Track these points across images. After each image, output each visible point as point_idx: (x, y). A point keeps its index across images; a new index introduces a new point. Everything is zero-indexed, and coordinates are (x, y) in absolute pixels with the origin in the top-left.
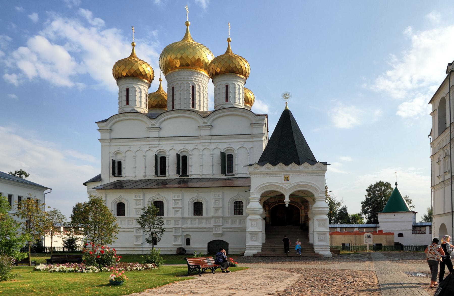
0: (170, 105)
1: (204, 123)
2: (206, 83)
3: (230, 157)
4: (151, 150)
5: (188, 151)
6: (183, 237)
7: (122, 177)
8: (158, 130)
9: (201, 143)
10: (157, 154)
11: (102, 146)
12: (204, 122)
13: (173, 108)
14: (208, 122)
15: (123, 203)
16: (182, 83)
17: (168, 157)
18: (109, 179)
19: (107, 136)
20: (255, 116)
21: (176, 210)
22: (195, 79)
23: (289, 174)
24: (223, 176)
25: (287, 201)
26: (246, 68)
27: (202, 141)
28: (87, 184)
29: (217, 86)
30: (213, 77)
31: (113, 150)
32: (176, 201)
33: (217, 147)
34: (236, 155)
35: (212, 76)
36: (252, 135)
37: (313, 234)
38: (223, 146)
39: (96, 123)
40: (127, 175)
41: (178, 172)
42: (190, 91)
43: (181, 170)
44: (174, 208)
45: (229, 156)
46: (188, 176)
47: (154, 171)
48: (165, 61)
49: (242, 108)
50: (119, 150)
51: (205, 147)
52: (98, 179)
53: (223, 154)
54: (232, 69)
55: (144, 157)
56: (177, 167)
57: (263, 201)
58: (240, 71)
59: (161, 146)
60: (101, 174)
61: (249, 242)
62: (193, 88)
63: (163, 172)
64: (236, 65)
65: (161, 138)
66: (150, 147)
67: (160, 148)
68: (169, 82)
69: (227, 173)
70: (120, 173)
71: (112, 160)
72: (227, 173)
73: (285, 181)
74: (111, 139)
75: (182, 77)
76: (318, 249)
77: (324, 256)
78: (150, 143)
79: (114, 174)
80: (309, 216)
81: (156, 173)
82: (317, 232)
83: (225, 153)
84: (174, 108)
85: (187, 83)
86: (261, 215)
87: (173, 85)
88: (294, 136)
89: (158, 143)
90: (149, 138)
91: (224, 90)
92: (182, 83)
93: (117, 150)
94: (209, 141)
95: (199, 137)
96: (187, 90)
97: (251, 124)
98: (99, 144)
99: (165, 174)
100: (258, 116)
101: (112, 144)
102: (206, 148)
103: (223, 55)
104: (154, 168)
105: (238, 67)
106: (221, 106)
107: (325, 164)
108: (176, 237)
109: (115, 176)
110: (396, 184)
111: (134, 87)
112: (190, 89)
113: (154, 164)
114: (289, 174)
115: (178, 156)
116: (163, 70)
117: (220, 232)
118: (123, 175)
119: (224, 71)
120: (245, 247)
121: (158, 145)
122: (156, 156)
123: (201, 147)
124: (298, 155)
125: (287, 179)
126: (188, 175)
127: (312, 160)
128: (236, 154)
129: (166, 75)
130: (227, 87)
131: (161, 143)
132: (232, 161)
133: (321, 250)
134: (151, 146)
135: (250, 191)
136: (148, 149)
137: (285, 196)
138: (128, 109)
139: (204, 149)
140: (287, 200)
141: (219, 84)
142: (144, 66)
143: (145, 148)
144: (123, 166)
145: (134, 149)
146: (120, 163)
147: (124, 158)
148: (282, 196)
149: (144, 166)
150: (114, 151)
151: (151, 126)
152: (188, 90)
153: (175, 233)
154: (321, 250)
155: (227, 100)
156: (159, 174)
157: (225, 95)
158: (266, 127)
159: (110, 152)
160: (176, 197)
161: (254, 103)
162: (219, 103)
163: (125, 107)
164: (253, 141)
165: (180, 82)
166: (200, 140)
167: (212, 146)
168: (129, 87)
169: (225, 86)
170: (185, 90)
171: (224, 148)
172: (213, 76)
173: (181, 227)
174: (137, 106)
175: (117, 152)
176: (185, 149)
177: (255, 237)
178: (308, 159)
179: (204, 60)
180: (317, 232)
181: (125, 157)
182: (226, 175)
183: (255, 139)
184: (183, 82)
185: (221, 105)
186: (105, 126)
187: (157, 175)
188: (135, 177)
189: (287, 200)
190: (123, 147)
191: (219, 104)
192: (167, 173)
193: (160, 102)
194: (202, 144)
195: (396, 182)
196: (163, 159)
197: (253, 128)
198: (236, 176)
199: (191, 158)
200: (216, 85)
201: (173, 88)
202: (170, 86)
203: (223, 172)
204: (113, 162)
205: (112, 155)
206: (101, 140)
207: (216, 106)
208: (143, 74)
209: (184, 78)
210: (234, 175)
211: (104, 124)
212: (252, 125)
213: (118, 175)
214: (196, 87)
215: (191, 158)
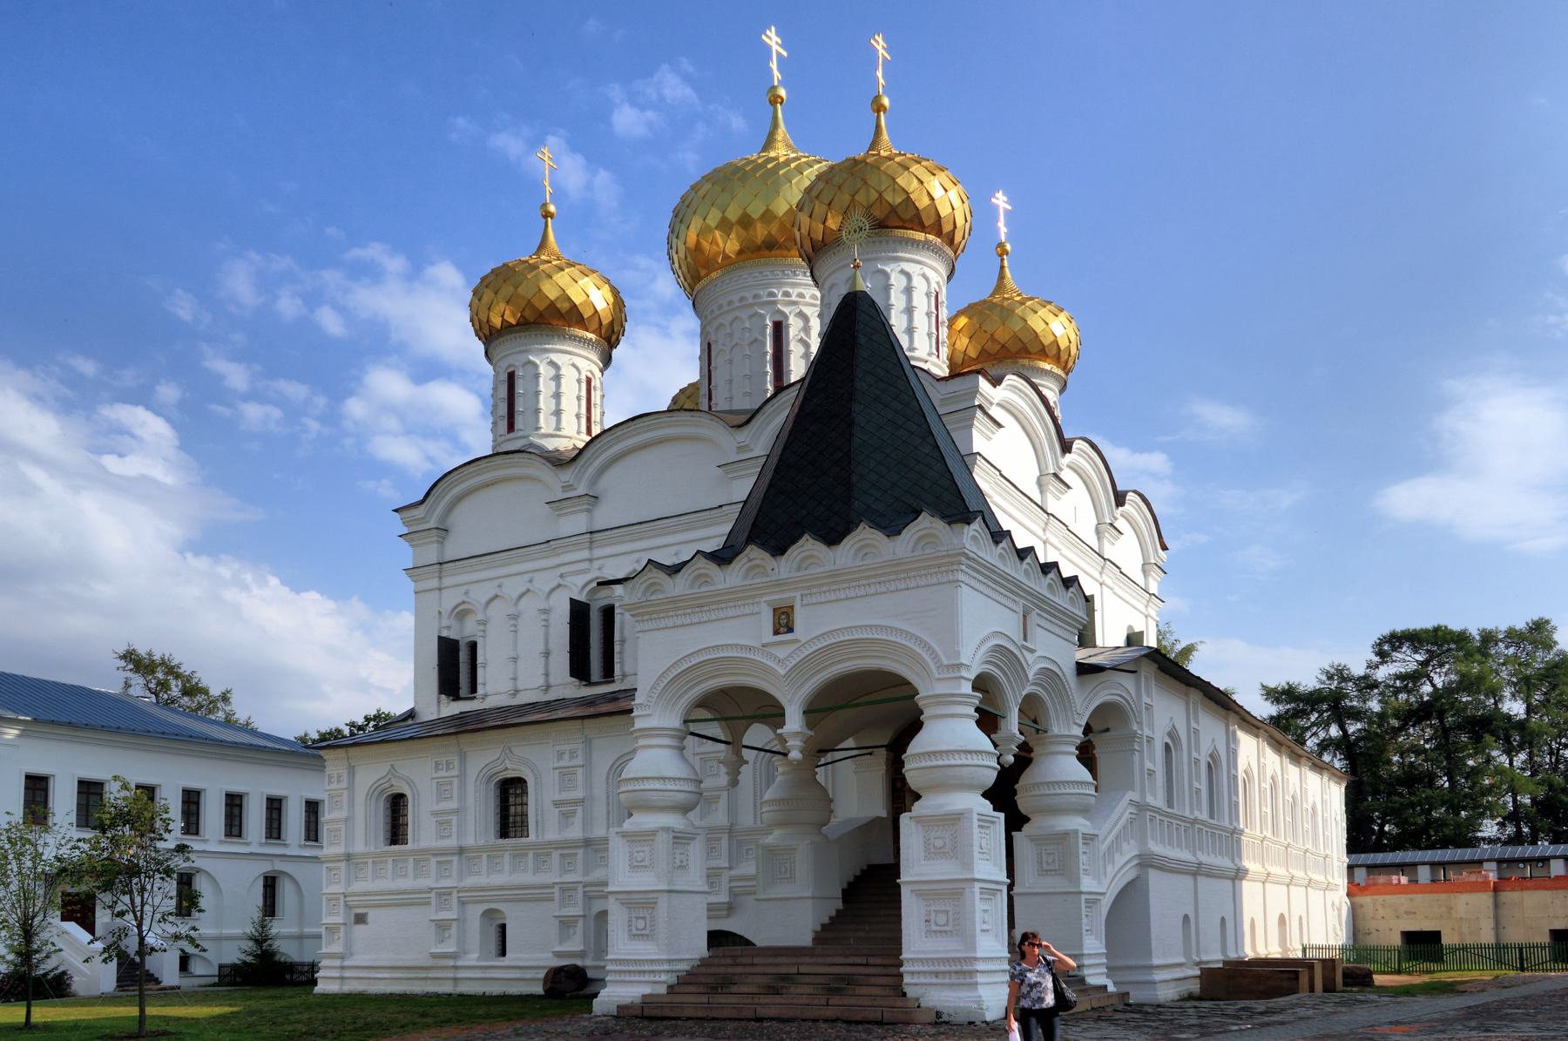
1: (741, 449)
6: (592, 924)
8: (586, 507)
12: (738, 448)
16: (736, 318)
21: (566, 810)
22: (787, 294)
23: (792, 594)
31: (451, 599)
32: (566, 775)
39: (396, 511)
40: (490, 689)
42: (764, 344)
44: (557, 804)
50: (466, 600)
55: (544, 617)
59: (596, 564)
61: (621, 946)
62: (779, 329)
65: (595, 535)
66: (561, 576)
73: (776, 633)
75: (735, 298)
76: (922, 980)
77: (945, 1018)
78: (561, 559)
82: (916, 887)
85: (751, 317)
89: (585, 554)
93: (460, 600)
101: (447, 581)
108: (566, 924)
111: (530, 362)
112: (764, 336)
114: (792, 594)
121: (586, 565)
125: (783, 622)
131: (597, 552)
133: (934, 980)
134: (563, 570)
136: (555, 584)
142: (562, 279)
143: (545, 582)
145: (513, 588)
146: (473, 647)
147: (481, 627)
149: (541, 648)
152: (756, 340)
153: (563, 905)
154: (934, 980)
159: (440, 613)
160: (566, 756)
163: (505, 441)
173: (580, 879)
174: (543, 431)
177: (644, 918)
180: (916, 887)
184: (737, 313)
186: (422, 520)
188: (515, 694)
190: (475, 587)
205: (445, 622)
208: (564, 306)
209: (742, 299)
211: (419, 512)
214: (788, 326)
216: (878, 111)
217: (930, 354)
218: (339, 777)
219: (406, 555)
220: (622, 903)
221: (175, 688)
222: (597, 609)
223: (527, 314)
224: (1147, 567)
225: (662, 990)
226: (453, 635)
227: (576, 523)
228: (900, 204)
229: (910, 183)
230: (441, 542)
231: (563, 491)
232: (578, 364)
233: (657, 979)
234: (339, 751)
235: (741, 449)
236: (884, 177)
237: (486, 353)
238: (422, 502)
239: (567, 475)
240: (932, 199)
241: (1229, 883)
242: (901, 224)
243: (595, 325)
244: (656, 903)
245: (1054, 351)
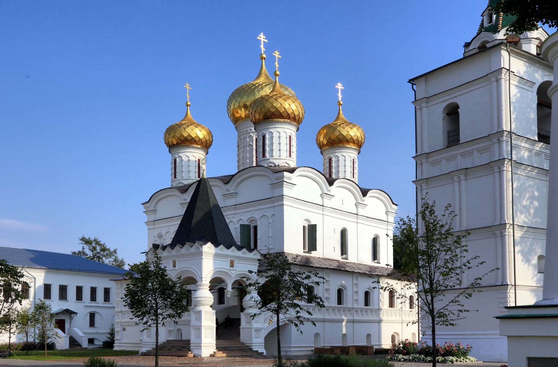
16: (245, 137)
31: (156, 232)
58: (277, 114)
75: (245, 130)
94: (234, 212)
120: (188, 343)
150: (157, 234)
159: (154, 236)
164: (274, 207)
166: (226, 212)
171: (247, 219)
175: (160, 234)
184: (245, 135)
186: (149, 207)
208: (189, 138)
211: (148, 205)
216: (276, 76)
217: (287, 157)
218: (119, 288)
219: (145, 218)
221: (98, 249)
223: (179, 141)
224: (387, 213)
226: (157, 243)
228: (275, 111)
229: (278, 104)
230: (155, 214)
232: (195, 155)
234: (118, 281)
236: (269, 103)
237: (169, 151)
238: (149, 202)
240: (285, 109)
241: (378, 324)
242: (276, 117)
243: (200, 142)
245: (352, 140)
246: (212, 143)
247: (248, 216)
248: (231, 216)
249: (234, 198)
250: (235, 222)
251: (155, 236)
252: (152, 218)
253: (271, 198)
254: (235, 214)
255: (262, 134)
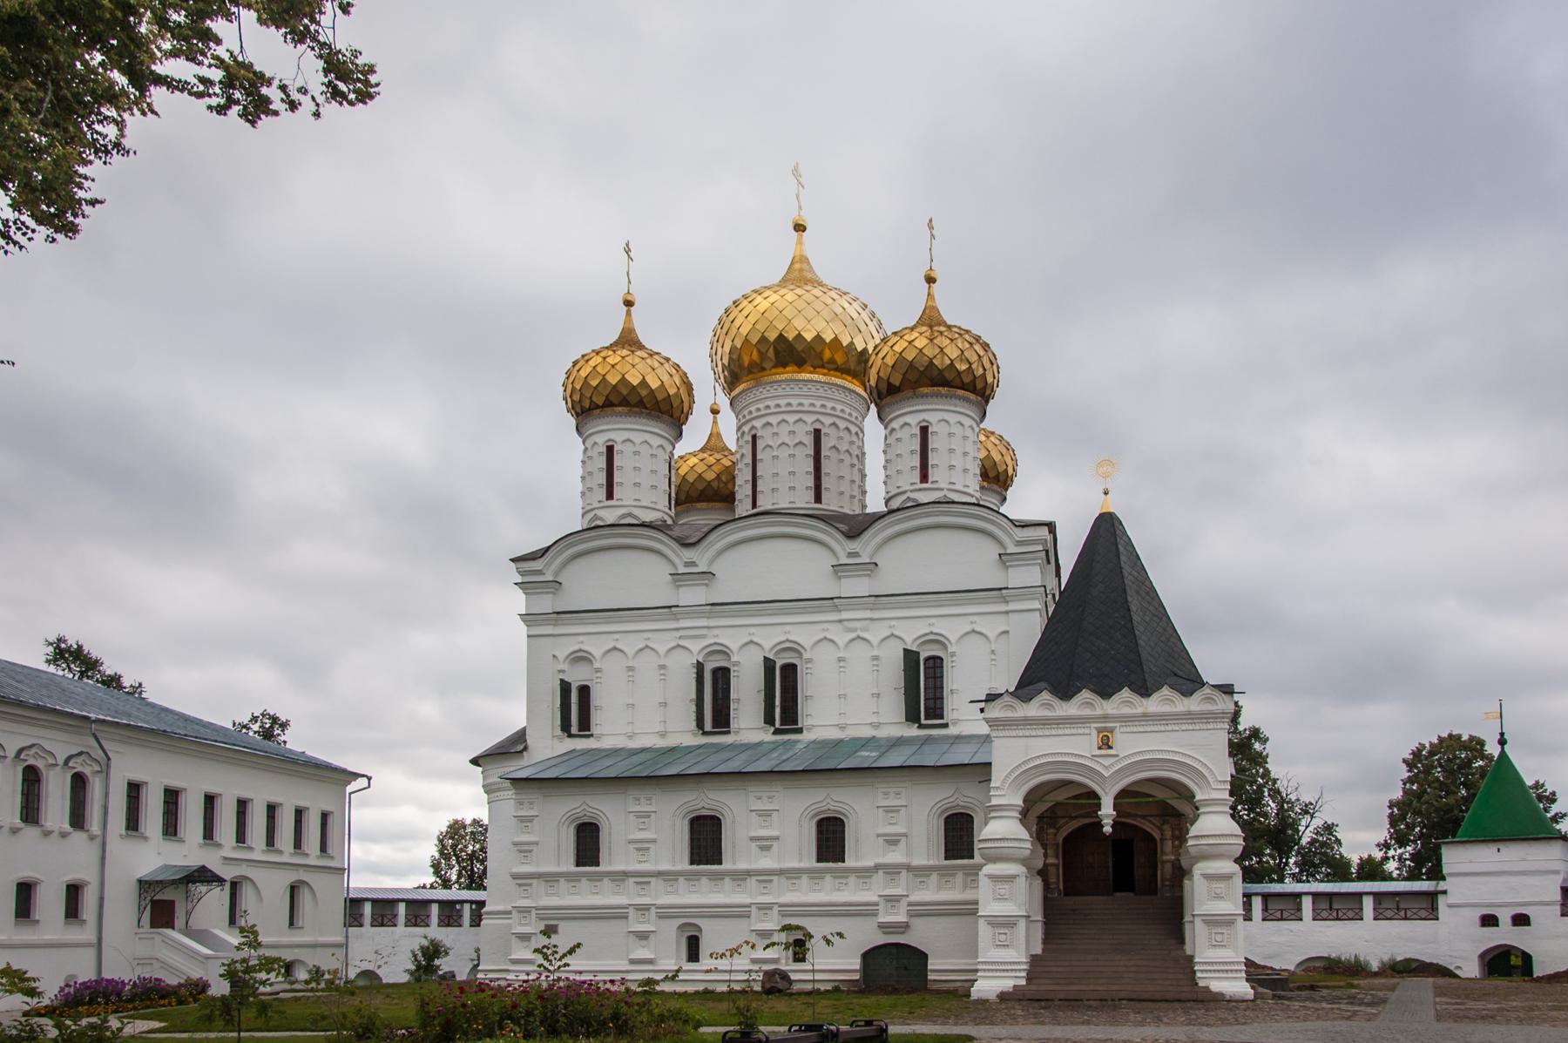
0: (743, 491)
2: (860, 419)
3: (935, 664)
4: (684, 647)
5: (802, 651)
7: (592, 735)
9: (840, 621)
10: (700, 660)
11: (529, 636)
13: (754, 505)
14: (865, 547)
15: (595, 824)
17: (736, 668)
18: (548, 747)
19: (546, 604)
20: (1012, 527)
24: (913, 731)
25: (1108, 816)
26: (985, 370)
27: (845, 615)
28: (480, 762)
29: (893, 430)
30: (878, 401)
31: (565, 648)
33: (893, 635)
34: (954, 659)
35: (876, 397)
36: (1003, 591)
37: (1192, 922)
38: (912, 631)
41: (769, 720)
43: (778, 711)
45: (931, 663)
46: (800, 731)
47: (694, 716)
48: (727, 349)
49: (973, 500)
51: (853, 635)
52: (514, 746)
53: (910, 657)
54: (941, 372)
56: (765, 701)
57: (1042, 807)
59: (716, 632)
60: (525, 728)
63: (722, 720)
64: (952, 361)
66: (680, 638)
67: (712, 641)
68: (740, 417)
69: (926, 719)
70: (585, 724)
71: (562, 680)
72: (926, 719)
74: (558, 613)
78: (682, 624)
79: (565, 726)
80: (1184, 863)
81: (700, 723)
83: (918, 653)
84: (758, 504)
86: (1024, 862)
87: (753, 427)
88: (1129, 599)
89: (703, 622)
90: (677, 606)
91: (917, 446)
92: (784, 421)
94: (867, 614)
95: (835, 601)
96: (797, 444)
97: (1000, 555)
98: (523, 629)
99: (727, 724)
100: (1023, 526)
102: (859, 637)
103: (912, 329)
104: (694, 708)
105: (958, 367)
106: (903, 497)
107: (1228, 690)
109: (570, 736)
110: (1502, 742)
113: (694, 696)
115: (769, 665)
116: (722, 379)
117: (902, 918)
118: (595, 730)
119: (915, 382)
121: (704, 632)
122: (700, 667)
123: (842, 638)
124: (1141, 663)
126: (800, 726)
127: (1188, 680)
128: (953, 654)
129: (733, 394)
130: (924, 431)
132: (942, 677)
134: (681, 633)
135: (990, 780)
136: (674, 644)
137: (1099, 798)
138: (610, 516)
139: (854, 639)
140: (1107, 811)
141: (895, 425)
144: (596, 699)
146: (585, 691)
148: (1091, 798)
151: (682, 570)
155: (924, 477)
156: (708, 726)
157: (916, 462)
158: (1049, 562)
161: (1015, 479)
162: (898, 487)
164: (1007, 612)
165: (774, 420)
167: (875, 634)
168: (613, 441)
169: (918, 432)
170: (791, 444)
172: (879, 398)
176: (791, 641)
178: (1175, 675)
179: (852, 343)
181: (598, 670)
182: (921, 726)
183: (1012, 606)
184: (786, 417)
185: (905, 492)
187: (703, 730)
189: (1107, 811)
191: (901, 490)
192: (734, 725)
193: (715, 485)
194: (846, 623)
195: (1502, 734)
196: (722, 677)
197: (1007, 567)
198: (952, 730)
199: (809, 671)
200: (889, 428)
201: (754, 437)
202: (744, 432)
203: (912, 716)
204: (565, 687)
206: (527, 617)
207: (890, 495)
210: (946, 726)
212: (1003, 557)
213: (579, 731)
215: (809, 671)
220: (989, 924)
222: (712, 667)
225: (1024, 982)
227: (693, 595)
231: (685, 566)
233: (1018, 974)
235: (851, 555)
239: (688, 554)
244: (1015, 924)
246: (687, 419)
247: (922, 628)
248: (858, 625)
249: (869, 575)
250: (875, 641)
251: (562, 655)
252: (546, 604)
253: (1000, 589)
254: (872, 619)
255: (920, 422)
